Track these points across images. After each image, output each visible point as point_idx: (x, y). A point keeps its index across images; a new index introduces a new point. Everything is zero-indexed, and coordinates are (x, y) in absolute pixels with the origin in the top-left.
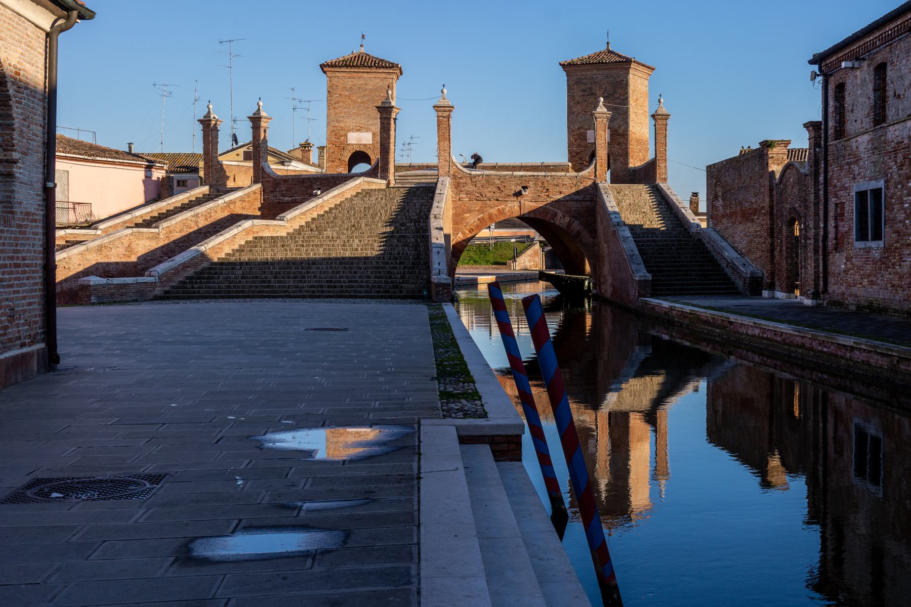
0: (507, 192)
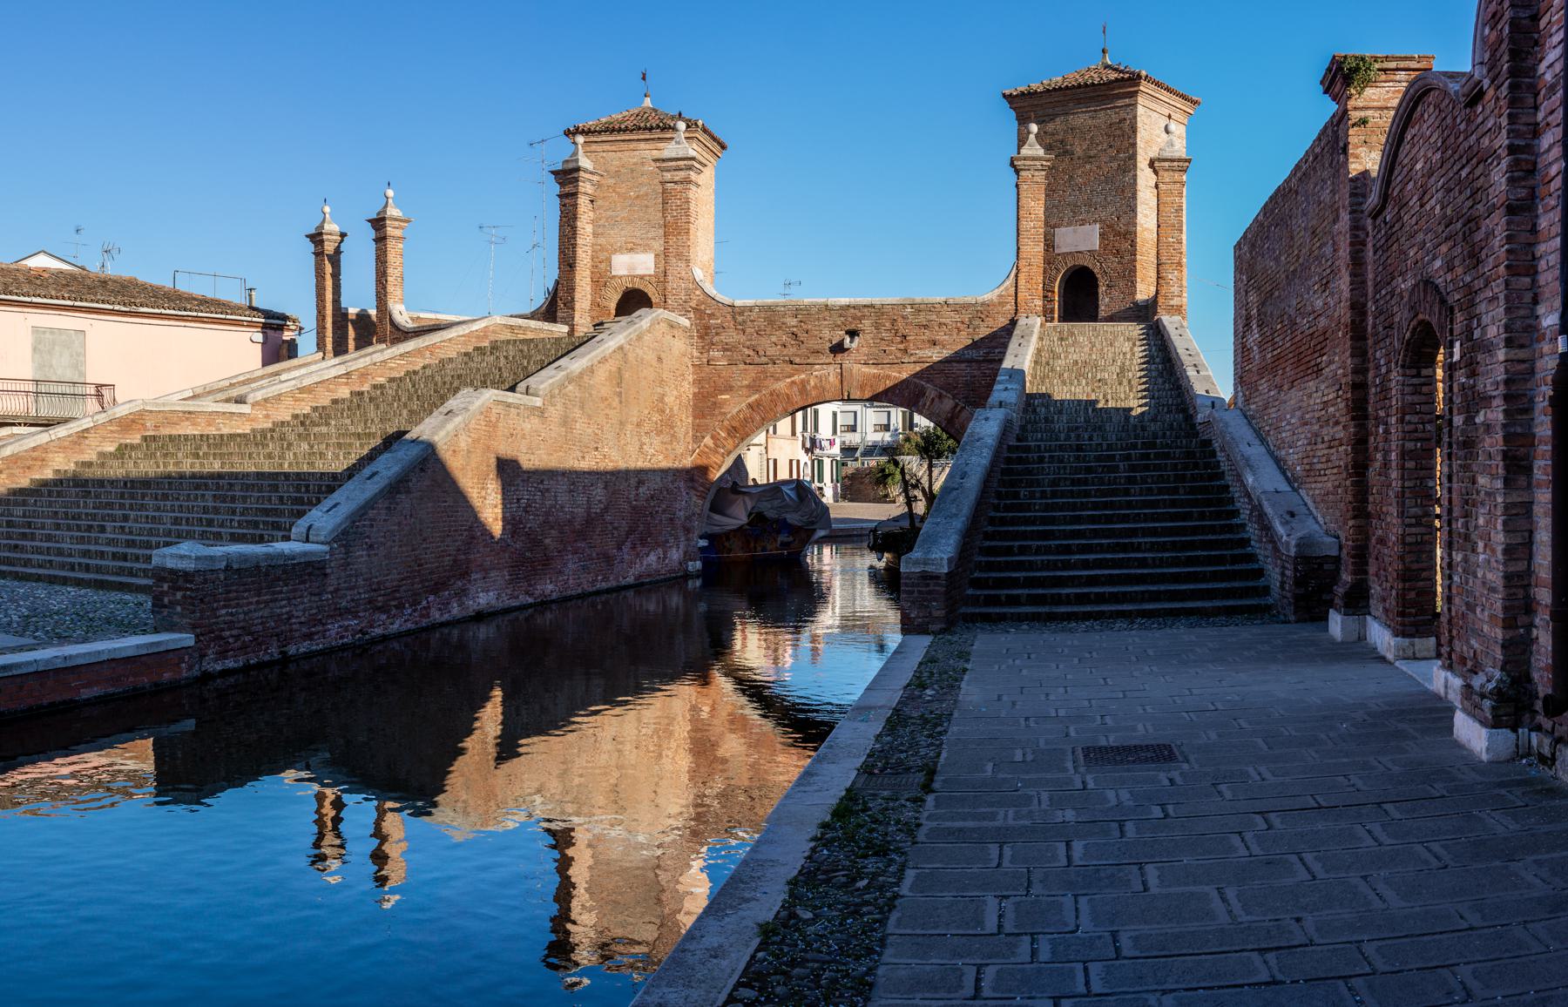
0: (812, 344)
